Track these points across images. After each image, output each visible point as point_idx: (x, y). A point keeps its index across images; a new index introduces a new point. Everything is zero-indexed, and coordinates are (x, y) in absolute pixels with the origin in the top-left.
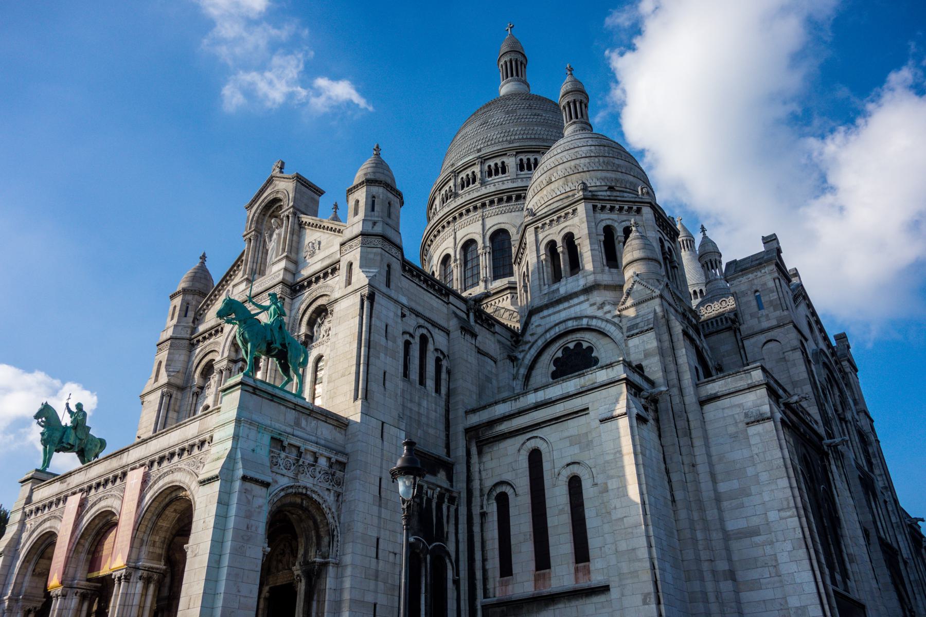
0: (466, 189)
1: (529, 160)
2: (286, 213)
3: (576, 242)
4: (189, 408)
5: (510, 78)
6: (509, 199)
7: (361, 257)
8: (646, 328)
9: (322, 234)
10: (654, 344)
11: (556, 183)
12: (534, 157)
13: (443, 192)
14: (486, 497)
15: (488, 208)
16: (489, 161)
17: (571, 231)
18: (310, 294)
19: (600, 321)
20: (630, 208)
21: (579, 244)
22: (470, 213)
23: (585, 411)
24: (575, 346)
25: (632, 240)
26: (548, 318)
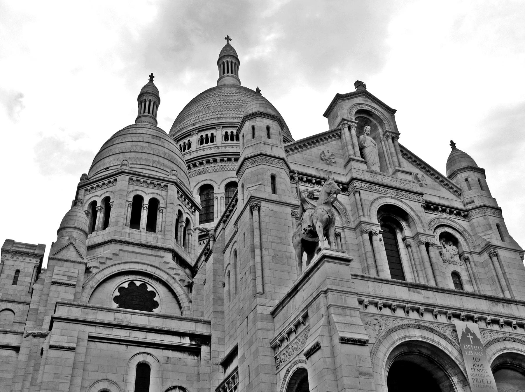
2: (393, 135)
5: (233, 75)
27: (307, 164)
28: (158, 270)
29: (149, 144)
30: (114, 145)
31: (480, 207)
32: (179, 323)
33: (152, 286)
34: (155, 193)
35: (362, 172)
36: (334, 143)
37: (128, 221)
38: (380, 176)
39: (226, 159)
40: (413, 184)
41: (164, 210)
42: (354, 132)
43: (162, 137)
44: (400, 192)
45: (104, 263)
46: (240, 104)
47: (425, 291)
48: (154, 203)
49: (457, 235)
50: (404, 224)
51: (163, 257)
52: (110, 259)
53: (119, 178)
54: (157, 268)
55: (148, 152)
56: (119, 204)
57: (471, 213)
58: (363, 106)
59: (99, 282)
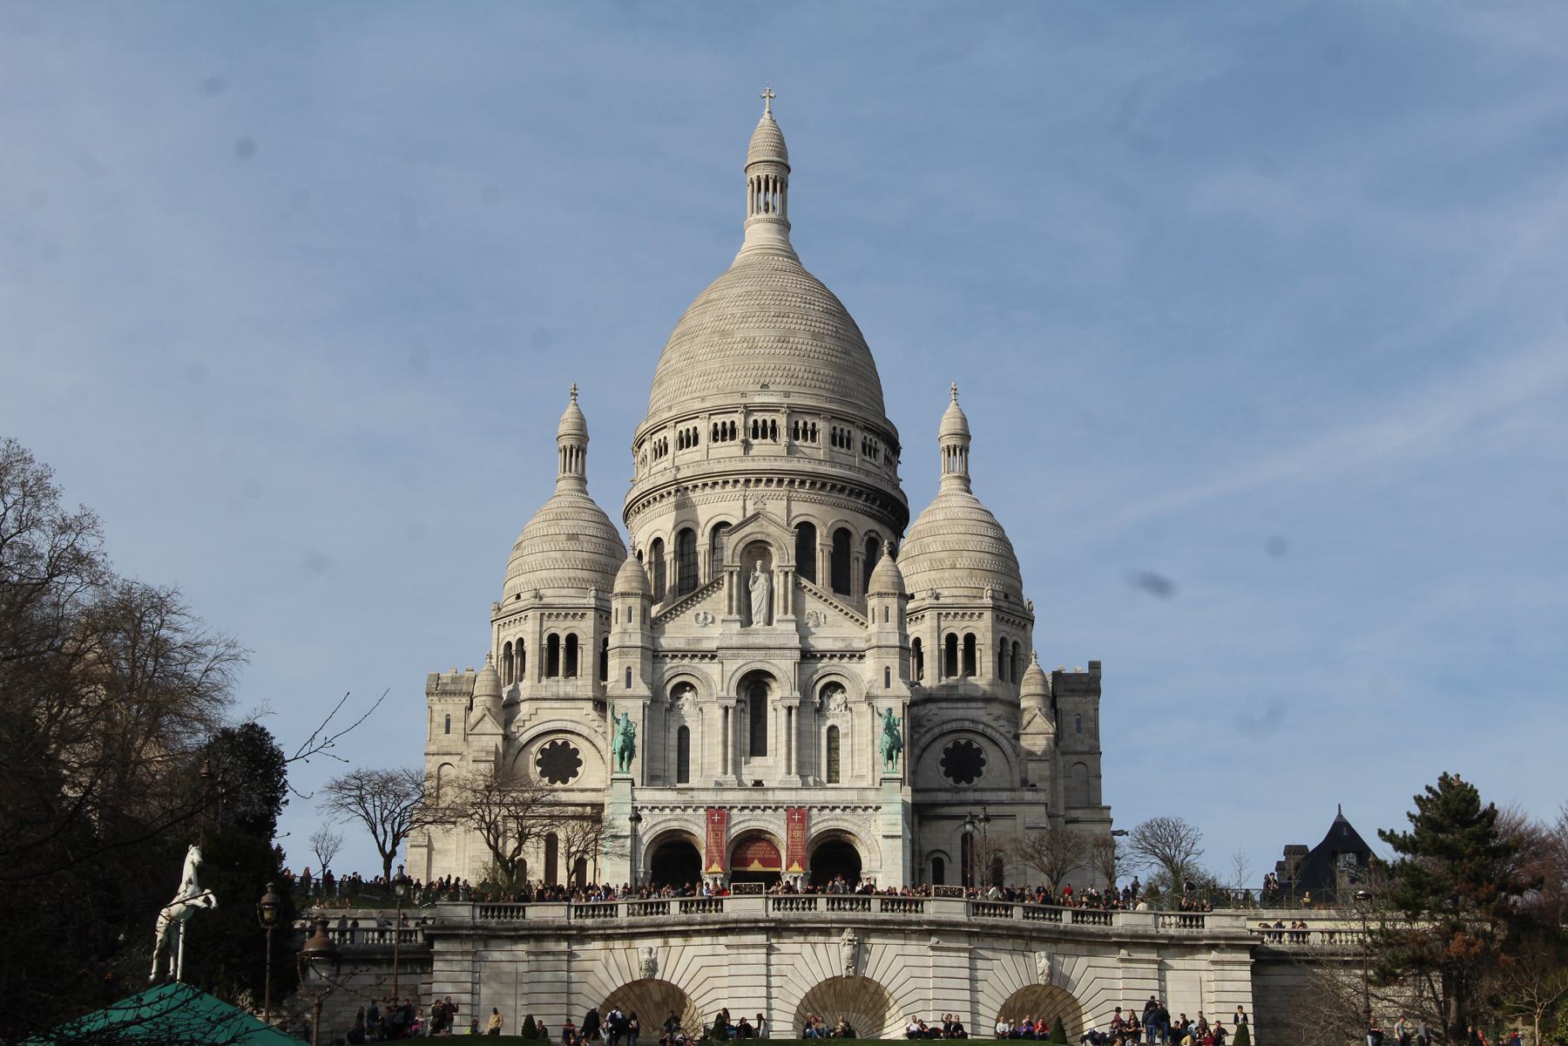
0: (760, 440)
1: (842, 430)
2: (786, 569)
6: (824, 485)
8: (1043, 758)
10: (1047, 773)
12: (849, 428)
13: (719, 420)
14: (924, 858)
16: (797, 414)
17: (975, 633)
19: (994, 732)
20: (1020, 623)
21: (981, 650)
22: (770, 484)
23: (1013, 816)
24: (966, 743)
25: (1035, 673)
26: (945, 711)
27: (678, 633)
32: (579, 794)
33: (575, 742)
38: (751, 636)
39: (710, 483)
41: (584, 647)
42: (735, 578)
45: (524, 726)
46: (742, 352)
48: (572, 640)
49: (845, 683)
50: (774, 685)
51: (583, 709)
52: (530, 720)
53: (530, 613)
55: (561, 567)
57: (867, 653)
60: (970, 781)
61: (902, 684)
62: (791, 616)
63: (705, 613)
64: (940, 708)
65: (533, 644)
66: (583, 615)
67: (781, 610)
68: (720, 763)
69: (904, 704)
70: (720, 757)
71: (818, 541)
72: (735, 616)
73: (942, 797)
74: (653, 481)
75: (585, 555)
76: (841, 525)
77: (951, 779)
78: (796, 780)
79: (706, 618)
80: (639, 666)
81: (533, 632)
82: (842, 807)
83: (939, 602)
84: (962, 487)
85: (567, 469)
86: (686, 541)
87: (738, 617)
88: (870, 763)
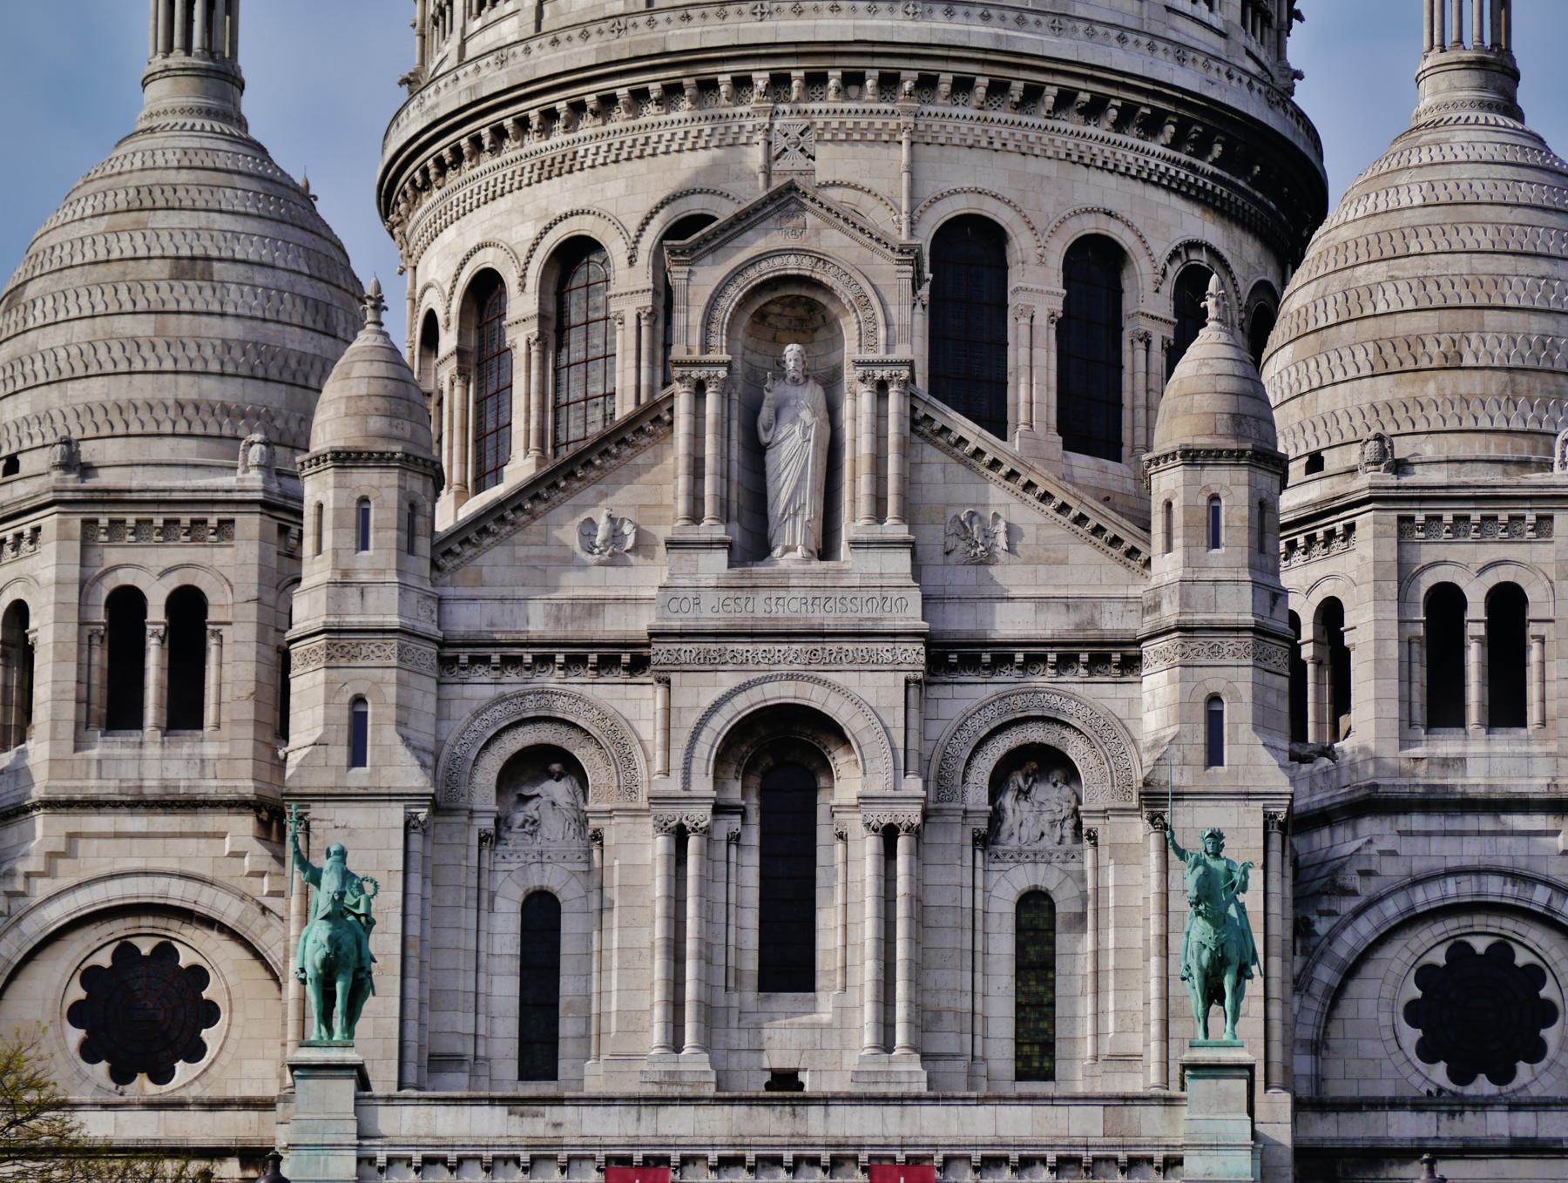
3: (1533, 629)
4: (474, 883)
6: (1033, 94)
7: (1255, 697)
9: (1015, 501)
11: (1477, 374)
15: (940, 106)
17: (1523, 585)
18: (1001, 699)
21: (1542, 640)
22: (853, 91)
24: (1490, 948)
26: (1421, 841)
28: (207, 890)
29: (159, 316)
30: (29, 330)
31: (1168, 632)
33: (194, 946)
34: (188, 566)
35: (691, 594)
36: (640, 459)
37: (94, 707)
38: (763, 594)
39: (655, 89)
40: (895, 594)
41: (225, 631)
43: (214, 253)
44: (828, 647)
45: (23, 895)
47: (556, 1110)
49: (1076, 750)
54: (202, 880)
55: (153, 366)
56: (56, 643)
57: (1148, 649)
58: (778, 261)
59: (12, 967)
60: (1503, 1076)
61: (1263, 749)
62: (893, 528)
63: (611, 519)
64: (1401, 833)
65: (57, 621)
66: (225, 528)
67: (864, 506)
68: (658, 1013)
69: (1269, 818)
70: (659, 994)
71: (1014, 281)
72: (710, 529)
73: (1405, 1127)
74: (472, 80)
75: (233, 329)
76: (1091, 225)
77: (1441, 1067)
78: (908, 1071)
79: (615, 536)
80: (391, 692)
81: (58, 583)
82: (1051, 1157)
83: (1405, 480)
84: (1489, 96)
85: (178, 40)
86: (578, 280)
87: (719, 532)
88: (1155, 1012)
